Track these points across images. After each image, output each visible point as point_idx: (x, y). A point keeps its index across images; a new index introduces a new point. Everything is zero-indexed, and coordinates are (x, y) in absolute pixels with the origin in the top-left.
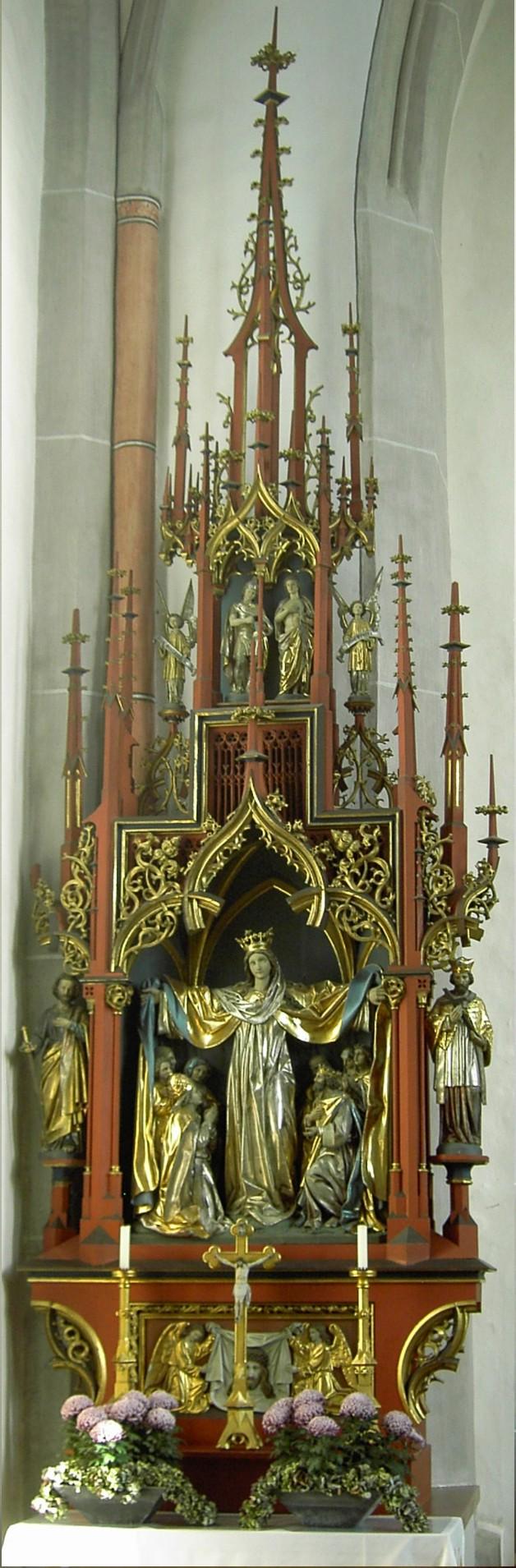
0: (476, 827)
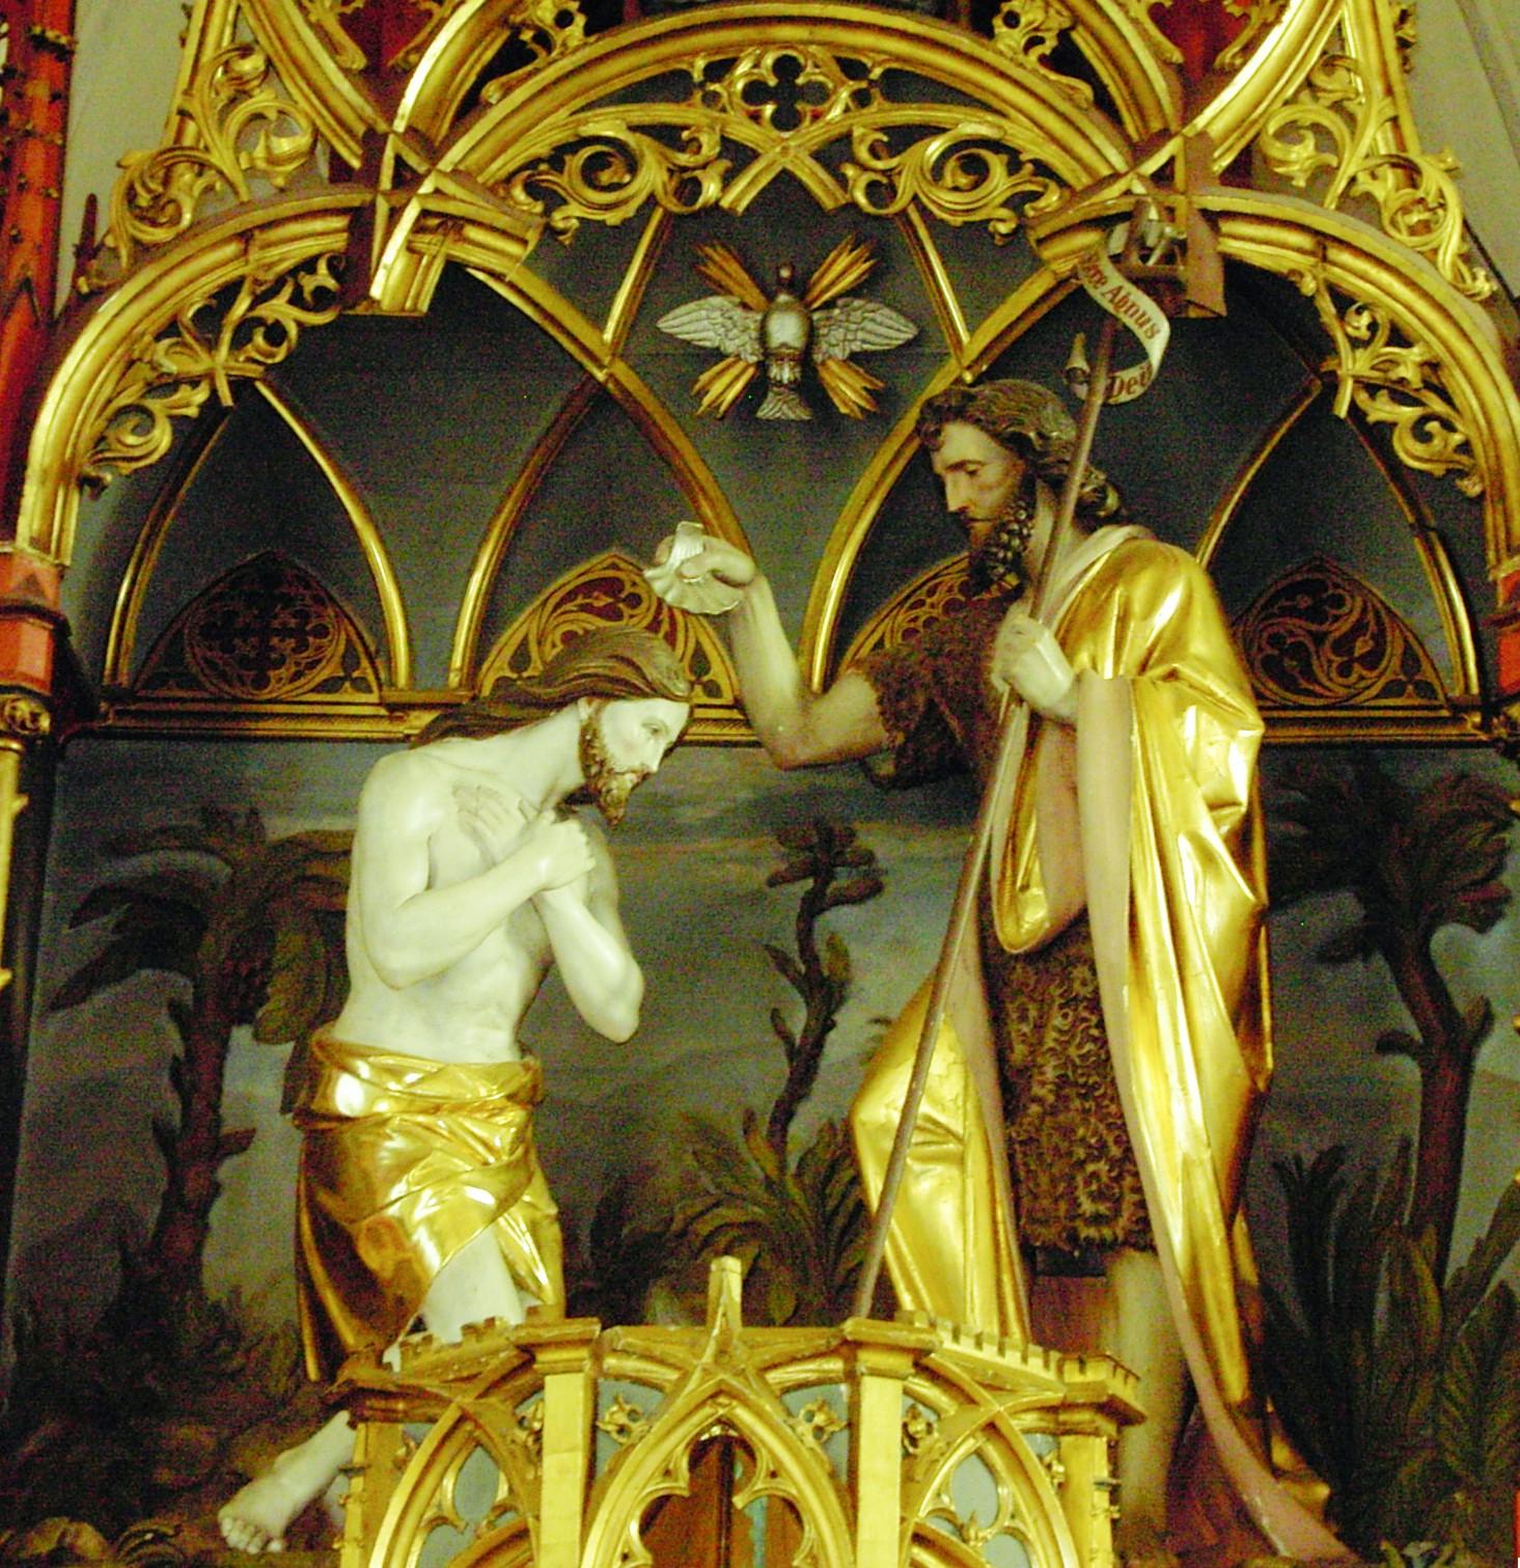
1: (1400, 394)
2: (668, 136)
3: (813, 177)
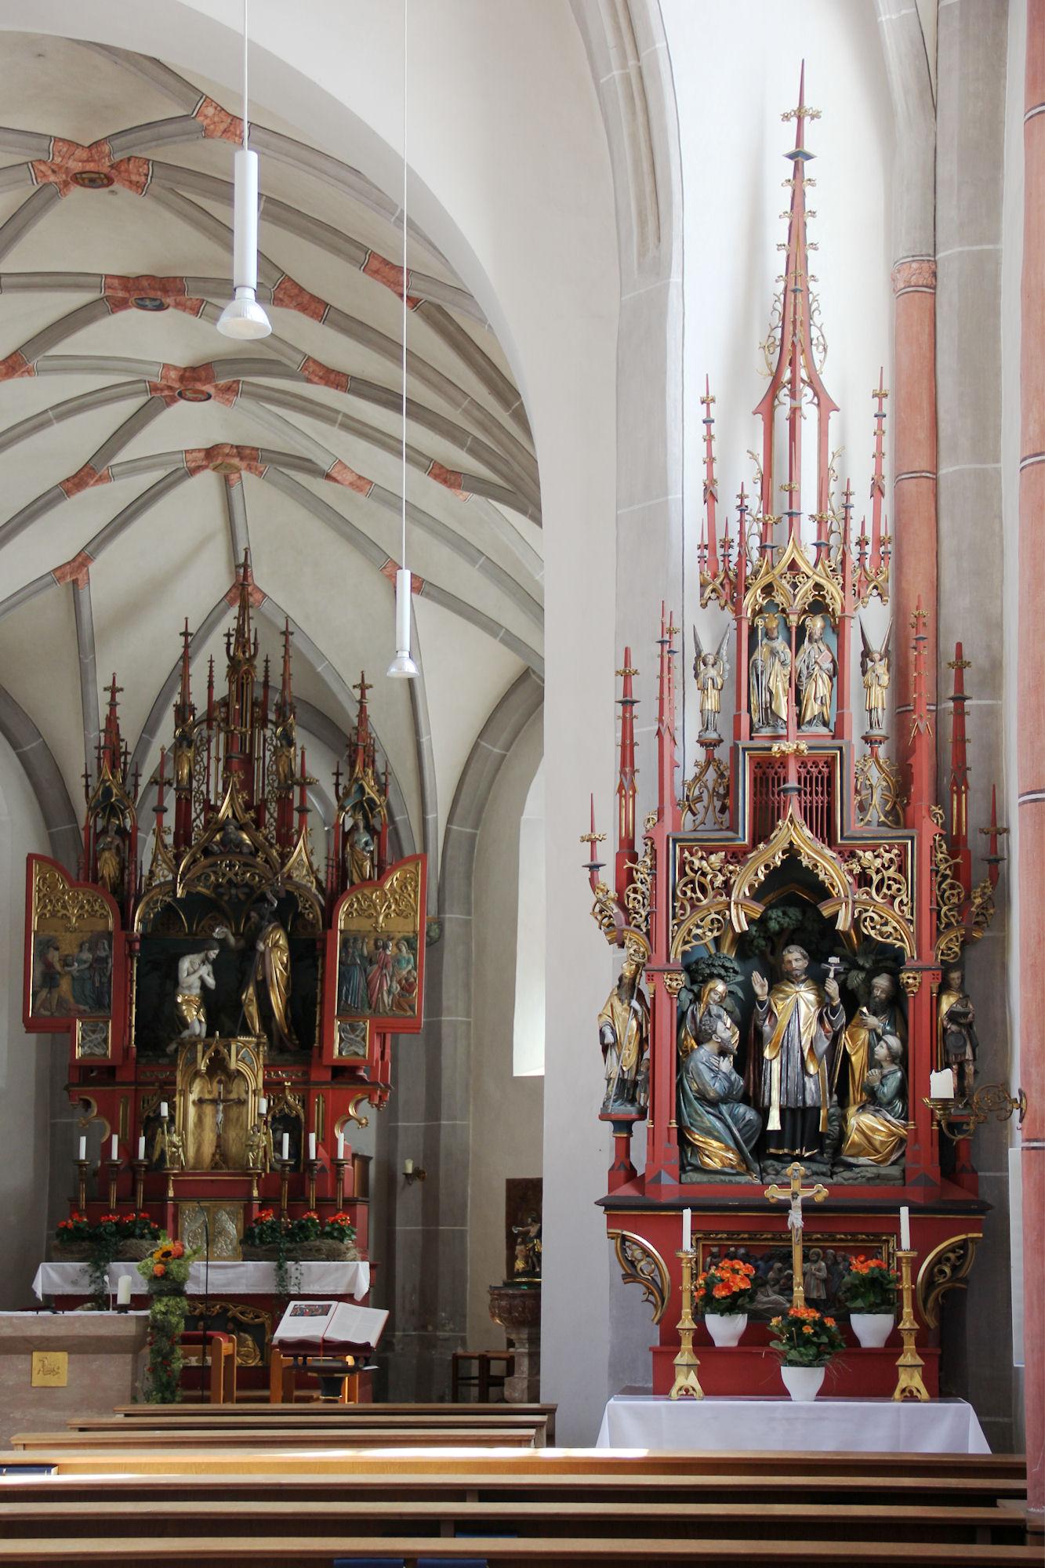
1: (306, 909)
2: (215, 873)
3: (233, 877)
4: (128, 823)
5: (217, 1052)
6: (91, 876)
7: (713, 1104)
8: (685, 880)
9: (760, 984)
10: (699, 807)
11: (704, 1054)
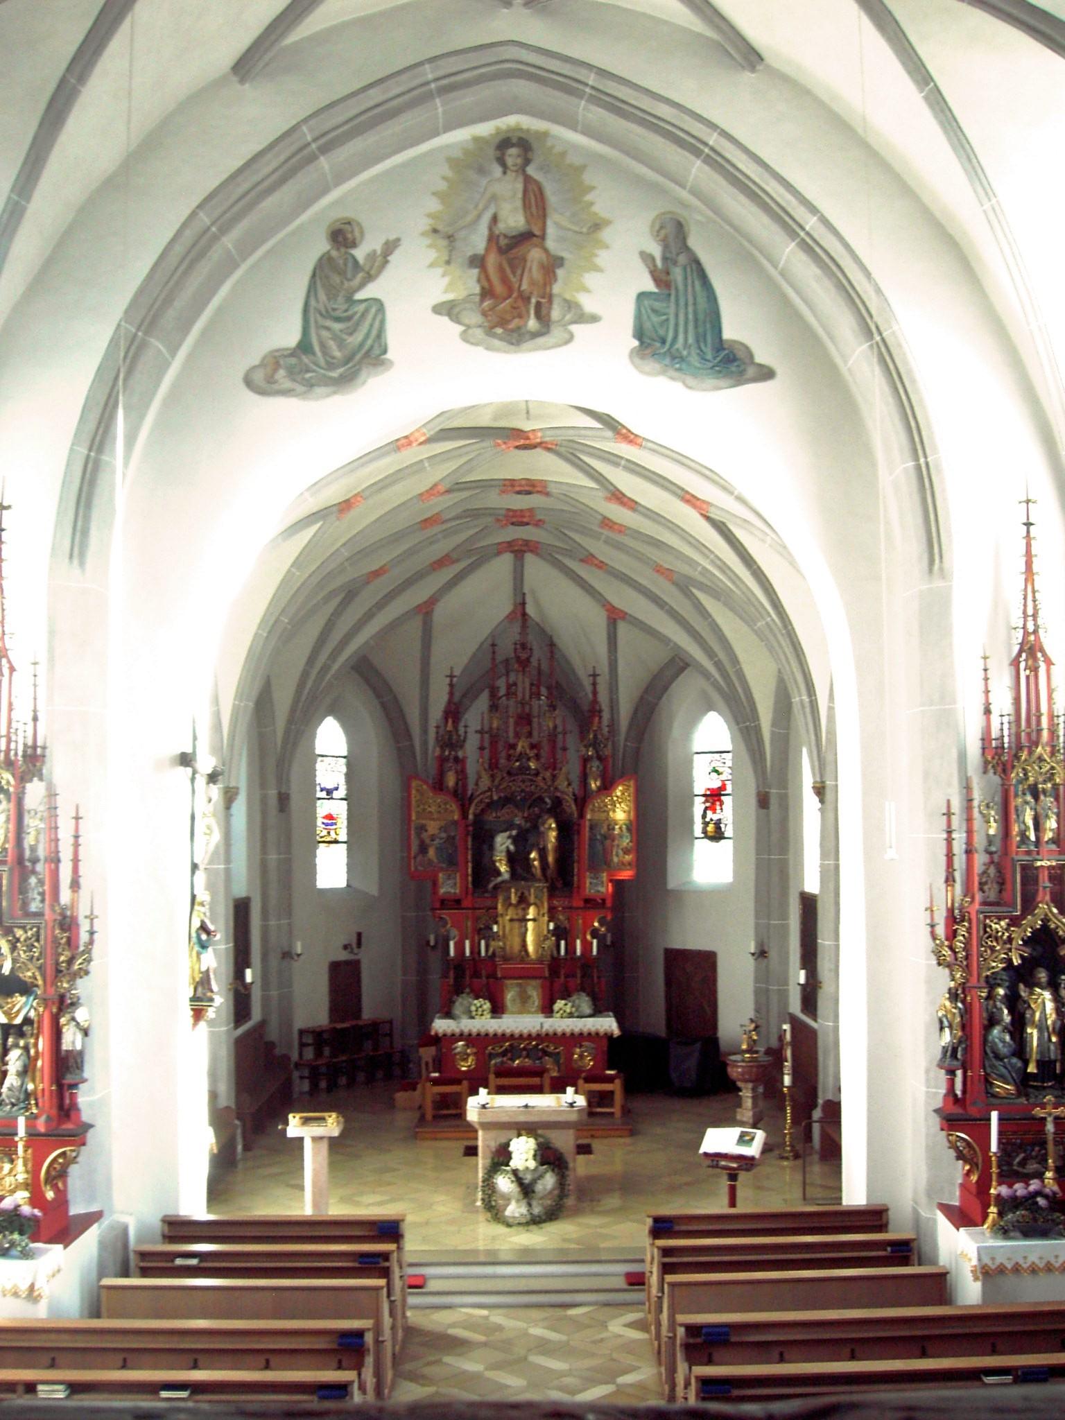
0: (84, 927)
4: (460, 754)
5: (523, 893)
6: (439, 786)
7: (1001, 1060)
8: (987, 935)
9: (1023, 992)
10: (986, 888)
11: (996, 1031)
